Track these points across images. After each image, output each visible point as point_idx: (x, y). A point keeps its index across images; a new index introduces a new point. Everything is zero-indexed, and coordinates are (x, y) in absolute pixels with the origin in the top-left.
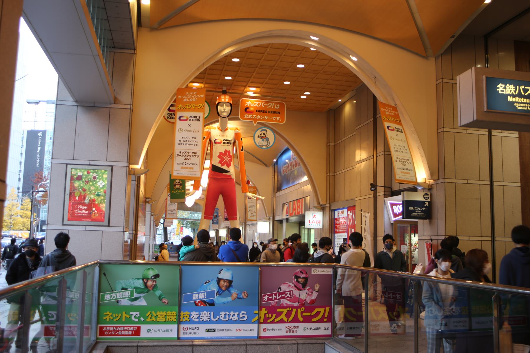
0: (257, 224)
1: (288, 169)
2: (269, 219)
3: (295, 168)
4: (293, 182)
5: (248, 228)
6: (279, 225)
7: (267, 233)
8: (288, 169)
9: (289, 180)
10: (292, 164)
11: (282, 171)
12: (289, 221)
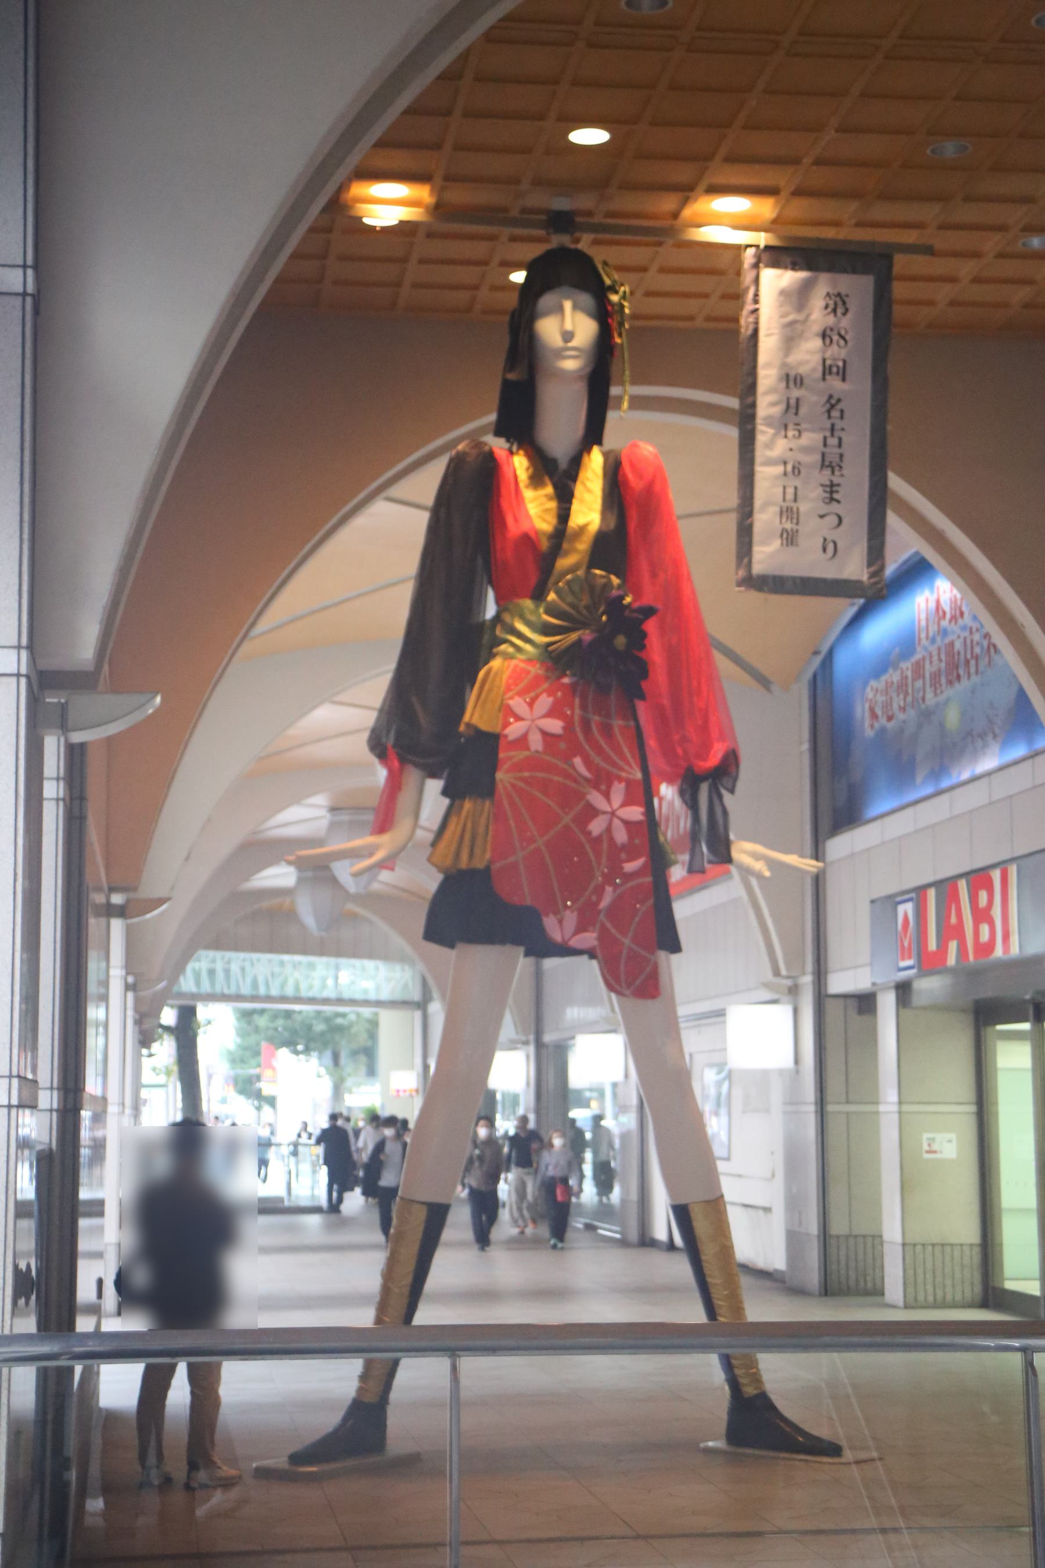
1: (898, 701)
2: (794, 991)
3: (949, 692)
8: (898, 701)
10: (928, 669)
11: (861, 711)
12: (917, 1000)
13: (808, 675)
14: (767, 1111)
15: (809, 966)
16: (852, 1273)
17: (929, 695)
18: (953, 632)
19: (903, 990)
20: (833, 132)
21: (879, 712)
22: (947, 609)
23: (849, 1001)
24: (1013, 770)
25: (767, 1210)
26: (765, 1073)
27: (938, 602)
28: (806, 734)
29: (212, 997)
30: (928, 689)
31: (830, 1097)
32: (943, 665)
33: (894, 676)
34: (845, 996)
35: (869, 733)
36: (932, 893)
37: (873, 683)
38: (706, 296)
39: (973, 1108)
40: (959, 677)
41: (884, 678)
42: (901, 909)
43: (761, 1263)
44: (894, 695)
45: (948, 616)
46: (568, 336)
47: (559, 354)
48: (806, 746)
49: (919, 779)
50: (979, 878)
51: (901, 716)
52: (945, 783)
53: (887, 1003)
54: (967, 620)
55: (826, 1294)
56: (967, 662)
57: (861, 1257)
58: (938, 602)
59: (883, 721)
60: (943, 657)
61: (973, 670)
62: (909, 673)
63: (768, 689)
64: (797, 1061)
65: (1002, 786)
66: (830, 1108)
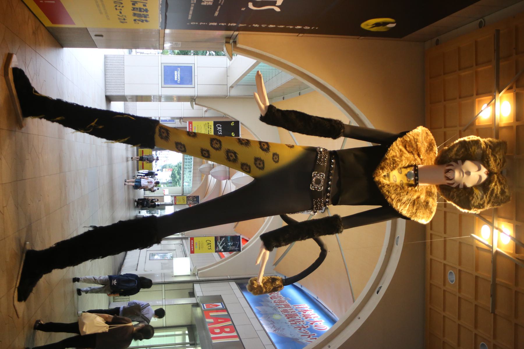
0: (186, 256)
2: (194, 275)
3: (284, 316)
4: (259, 312)
5: (178, 242)
6: (187, 292)
7: (173, 272)
12: (194, 308)
15: (201, 279)
19: (196, 305)
24: (268, 338)
25: (137, 270)
26: (172, 268)
31: (166, 285)
33: (283, 299)
38: (445, 233)
39: (164, 325)
40: (288, 318)
42: (220, 304)
43: (123, 269)
50: (233, 328)
51: (273, 301)
52: (258, 315)
53: (193, 300)
54: (305, 320)
56: (294, 321)
61: (292, 322)
64: (175, 276)
65: (261, 334)
66: (163, 286)
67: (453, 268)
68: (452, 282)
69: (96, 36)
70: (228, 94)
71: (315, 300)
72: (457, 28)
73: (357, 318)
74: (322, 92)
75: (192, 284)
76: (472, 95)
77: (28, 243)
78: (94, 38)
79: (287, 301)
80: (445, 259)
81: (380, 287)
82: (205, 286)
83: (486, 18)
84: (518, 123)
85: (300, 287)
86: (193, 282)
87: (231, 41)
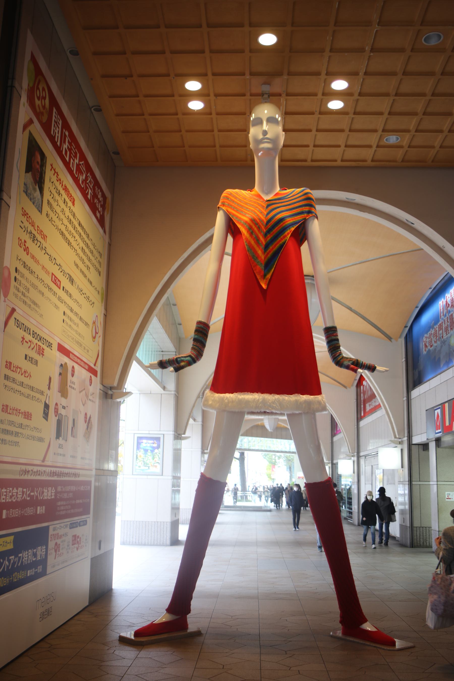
1: (434, 339)
2: (400, 443)
5: (362, 461)
7: (397, 470)
8: (434, 339)
9: (439, 360)
11: (422, 346)
12: (443, 445)
13: (404, 335)
14: (394, 484)
15: (406, 434)
16: (421, 540)
17: (444, 335)
18: (452, 311)
19: (438, 441)
20: (377, 26)
21: (427, 345)
22: (450, 303)
23: (420, 446)
26: (393, 470)
27: (446, 301)
28: (404, 356)
29: (249, 450)
30: (444, 333)
31: (413, 479)
32: (449, 323)
33: (433, 331)
34: (418, 445)
35: (425, 353)
36: (447, 405)
37: (426, 335)
38: (339, 146)
41: (429, 333)
42: (436, 412)
44: (433, 338)
45: (450, 306)
46: (265, 133)
47: (261, 142)
48: (404, 359)
49: (441, 366)
51: (435, 345)
53: (432, 446)
55: (412, 547)
57: (425, 534)
58: (446, 301)
59: (429, 347)
60: (449, 321)
62: (437, 329)
63: (391, 341)
66: (413, 483)
67: (381, 138)
68: (397, 139)
69: (100, 548)
70: (173, 393)
71: (434, 291)
72: (101, 133)
73: (445, 249)
74: (172, 286)
75: (413, 446)
76: (178, 119)
77: (331, 633)
78: (102, 551)
79: (435, 327)
80: (370, 146)
81: (407, 220)
82: (415, 429)
83: (91, 104)
84: (210, 74)
85: (418, 310)
86: (410, 445)
87: (110, 392)
